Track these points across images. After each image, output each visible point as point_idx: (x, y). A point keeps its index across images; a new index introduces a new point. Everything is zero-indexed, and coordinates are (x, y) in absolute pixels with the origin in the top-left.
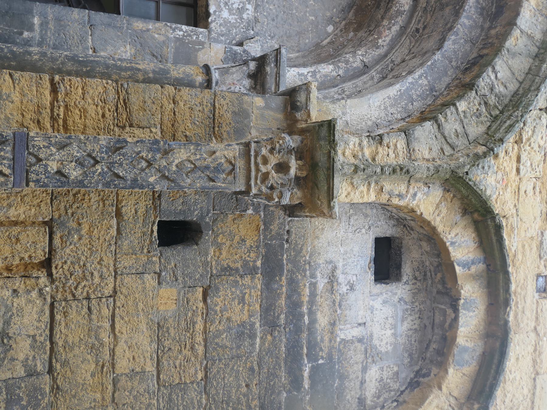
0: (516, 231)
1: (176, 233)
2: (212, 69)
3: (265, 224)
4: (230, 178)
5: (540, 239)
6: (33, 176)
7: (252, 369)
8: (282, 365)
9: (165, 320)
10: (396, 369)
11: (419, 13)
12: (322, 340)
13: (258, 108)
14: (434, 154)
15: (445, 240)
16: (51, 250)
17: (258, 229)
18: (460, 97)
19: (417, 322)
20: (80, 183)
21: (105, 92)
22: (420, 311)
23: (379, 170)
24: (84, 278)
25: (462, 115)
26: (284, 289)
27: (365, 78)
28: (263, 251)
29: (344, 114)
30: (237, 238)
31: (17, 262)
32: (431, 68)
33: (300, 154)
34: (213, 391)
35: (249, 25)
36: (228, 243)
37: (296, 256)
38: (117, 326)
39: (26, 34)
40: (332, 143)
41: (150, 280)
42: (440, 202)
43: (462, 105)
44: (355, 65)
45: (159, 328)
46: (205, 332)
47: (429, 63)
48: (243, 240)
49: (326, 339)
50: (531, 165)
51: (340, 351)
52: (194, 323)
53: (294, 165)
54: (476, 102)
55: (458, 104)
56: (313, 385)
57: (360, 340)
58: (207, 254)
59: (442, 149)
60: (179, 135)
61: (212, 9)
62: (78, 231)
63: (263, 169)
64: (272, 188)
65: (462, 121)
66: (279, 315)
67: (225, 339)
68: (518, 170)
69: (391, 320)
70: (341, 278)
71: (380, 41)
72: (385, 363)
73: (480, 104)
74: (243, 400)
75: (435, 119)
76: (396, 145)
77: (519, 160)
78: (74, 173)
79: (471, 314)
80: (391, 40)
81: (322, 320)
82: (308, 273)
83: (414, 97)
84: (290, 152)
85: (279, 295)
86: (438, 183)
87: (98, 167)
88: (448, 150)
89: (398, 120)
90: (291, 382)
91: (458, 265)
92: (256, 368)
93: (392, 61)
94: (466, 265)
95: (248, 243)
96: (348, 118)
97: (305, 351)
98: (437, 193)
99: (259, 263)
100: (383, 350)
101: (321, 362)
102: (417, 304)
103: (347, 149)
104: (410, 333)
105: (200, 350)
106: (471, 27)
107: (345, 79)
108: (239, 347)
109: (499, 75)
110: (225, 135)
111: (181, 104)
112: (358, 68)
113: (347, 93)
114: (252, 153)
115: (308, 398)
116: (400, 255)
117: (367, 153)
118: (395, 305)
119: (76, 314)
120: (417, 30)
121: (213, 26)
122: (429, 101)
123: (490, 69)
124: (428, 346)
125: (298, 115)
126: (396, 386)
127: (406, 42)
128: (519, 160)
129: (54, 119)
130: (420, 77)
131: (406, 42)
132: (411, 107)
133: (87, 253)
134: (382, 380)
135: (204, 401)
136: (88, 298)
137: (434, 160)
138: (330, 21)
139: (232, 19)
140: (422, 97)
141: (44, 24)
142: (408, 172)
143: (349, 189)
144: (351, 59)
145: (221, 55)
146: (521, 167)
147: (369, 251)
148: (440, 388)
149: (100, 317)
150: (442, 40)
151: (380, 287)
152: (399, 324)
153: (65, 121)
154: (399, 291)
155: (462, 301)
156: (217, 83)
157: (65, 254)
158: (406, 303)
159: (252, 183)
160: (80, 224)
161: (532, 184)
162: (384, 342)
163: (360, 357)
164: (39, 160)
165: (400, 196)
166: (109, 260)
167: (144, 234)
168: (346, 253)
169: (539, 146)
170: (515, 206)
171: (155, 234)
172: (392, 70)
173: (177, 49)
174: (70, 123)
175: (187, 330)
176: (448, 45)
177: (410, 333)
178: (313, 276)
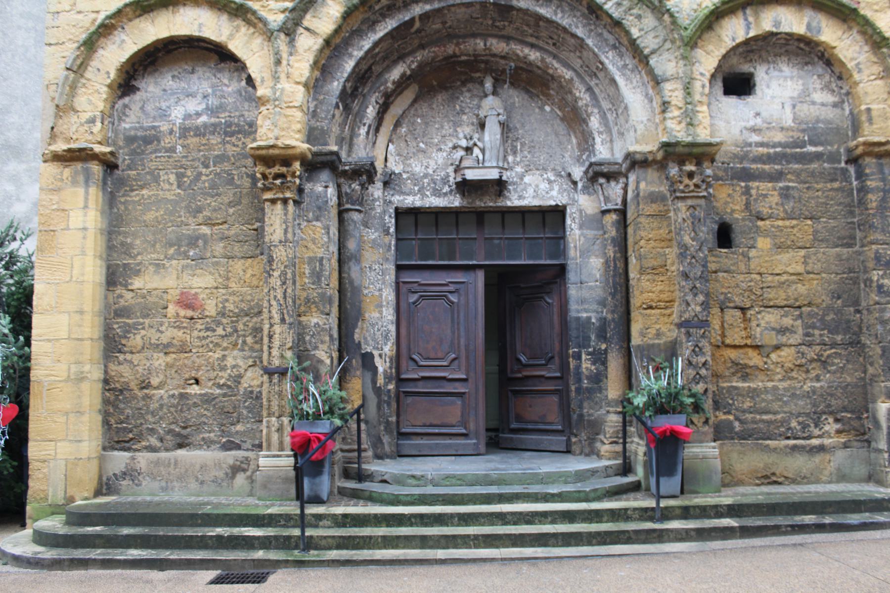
1: (725, 236)
2: (605, 208)
3: (718, 180)
4: (698, 209)
6: (704, 318)
7: (808, 188)
8: (806, 167)
9: (776, 244)
10: (815, 77)
11: (541, 43)
12: (792, 137)
13: (647, 185)
14: (672, 58)
15: (731, 46)
16: (736, 308)
17: (721, 185)
18: (628, 33)
19: (783, 58)
20: (707, 295)
21: (648, 280)
22: (775, 56)
23: (690, 107)
24: (751, 291)
25: (643, 33)
26: (759, 166)
27: (597, 90)
28: (735, 182)
29: (642, 122)
30: (729, 200)
31: (742, 325)
32: (599, 49)
33: (681, 162)
34: (819, 214)
35: (558, 176)
36: (731, 205)
37: (738, 158)
38: (778, 272)
39: (593, 320)
40: (677, 144)
41: (753, 253)
42: (705, 51)
43: (635, 33)
44: (588, 99)
45: (780, 247)
46: (783, 219)
47: (596, 50)
48: (729, 195)
49: (791, 134)
51: (800, 124)
52: (778, 226)
53: (690, 167)
54: (631, 18)
55: (635, 37)
56: (821, 144)
57: (794, 106)
58: (737, 219)
59: (668, 50)
60: (668, 237)
61: (553, 203)
62: (726, 294)
63: (692, 188)
64: (703, 181)
65: (646, 33)
66: (776, 170)
67: (789, 206)
69: (781, 82)
70: (751, 123)
71: (567, 77)
72: (811, 86)
73: (631, 15)
74: (826, 194)
75: (647, 57)
76: (670, 91)
78: (701, 298)
79: (783, 20)
80: (564, 66)
81: (779, 137)
82: (749, 149)
83: (623, 63)
84: (681, 170)
85: (763, 170)
86: (693, 53)
87: (698, 285)
88: (668, 45)
89: (641, 77)
90: (818, 160)
91: (748, 33)
92: (807, 185)
93: (581, 67)
94: (748, 27)
95: (731, 192)
96: (645, 119)
97: (798, 150)
98: (699, 53)
99: (743, 184)
100: (801, 87)
101: (806, 138)
102: (770, 59)
103: (678, 132)
104: (791, 65)
105: (794, 222)
106: (562, 12)
107: (599, 107)
108: (794, 197)
110: (666, 208)
111: (650, 236)
112: (590, 96)
113: (611, 106)
114: (683, 195)
115: (829, 148)
116: (735, 73)
117: (676, 113)
118: (771, 78)
119: (771, 294)
120: (554, 44)
121: (564, 202)
122: (623, 50)
123: (606, 7)
124: (802, 49)
125: (650, 158)
126: (827, 77)
127: (563, 55)
129: (666, 308)
130: (607, 58)
131: (563, 55)
132: (630, 66)
133: (738, 289)
134: (822, 89)
135: (824, 220)
136: (762, 288)
137: (676, 58)
138: (541, 108)
139: (556, 188)
140: (621, 56)
141: (586, 311)
142: (689, 83)
143: (701, 127)
144: (584, 102)
145: (586, 197)
147: (733, 100)
148: (835, 48)
149: (772, 282)
150: (574, 36)
151: (758, 89)
152: (783, 74)
153: (667, 302)
154: (762, 75)
155: (774, 30)
156: (617, 204)
157: (738, 300)
158: (769, 69)
159: (701, 194)
160: (722, 293)
162: (796, 87)
163: (805, 107)
164: (696, 315)
165: (703, 86)
166: (741, 277)
167: (726, 257)
168: (735, 120)
171: (725, 250)
172: (587, 67)
173: (588, 228)
174: (667, 299)
175: (782, 231)
176: (580, 32)
177: (791, 65)
178: (750, 145)
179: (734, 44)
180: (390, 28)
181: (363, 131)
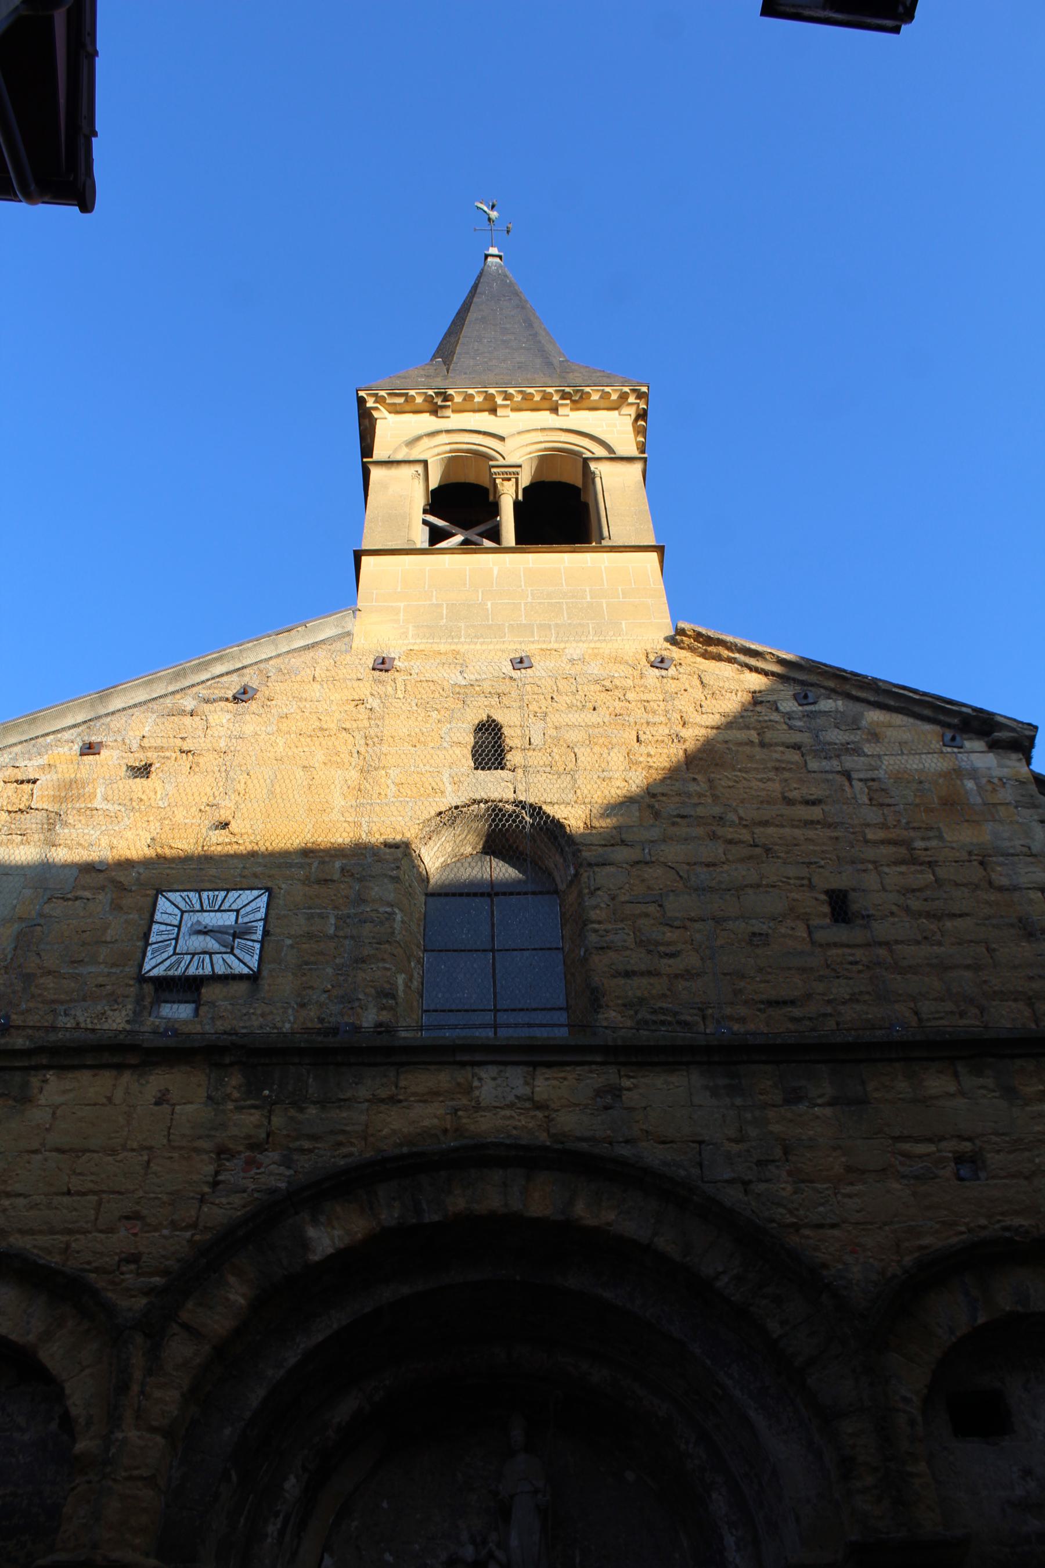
0: (913, 1223)
5: (912, 1182)
47: (708, 1362)
50: (822, 1204)
68: (833, 1226)
77: (820, 1226)
109: (720, 1269)
123: (719, 1284)
128: (820, 1226)
146: (828, 1221)
155: (1020, 1309)
161: (846, 1200)
169: (795, 1193)
170: (880, 1228)
179: (954, 1339)
180: (335, 1326)
181: (272, 1529)
